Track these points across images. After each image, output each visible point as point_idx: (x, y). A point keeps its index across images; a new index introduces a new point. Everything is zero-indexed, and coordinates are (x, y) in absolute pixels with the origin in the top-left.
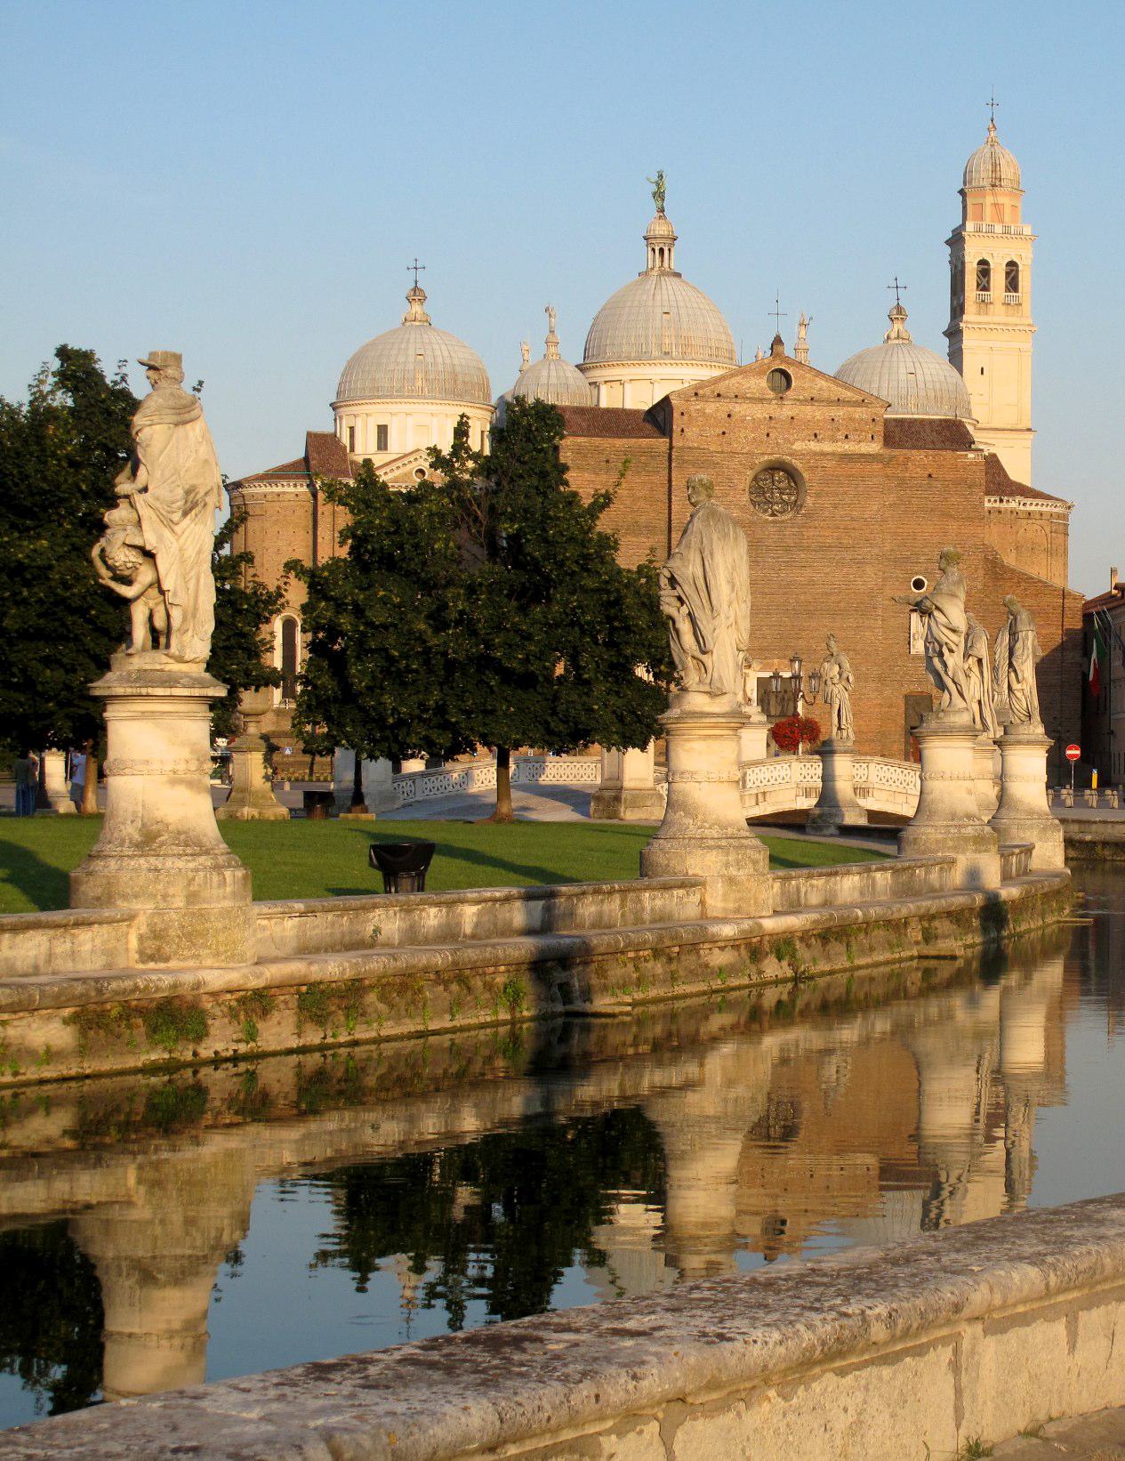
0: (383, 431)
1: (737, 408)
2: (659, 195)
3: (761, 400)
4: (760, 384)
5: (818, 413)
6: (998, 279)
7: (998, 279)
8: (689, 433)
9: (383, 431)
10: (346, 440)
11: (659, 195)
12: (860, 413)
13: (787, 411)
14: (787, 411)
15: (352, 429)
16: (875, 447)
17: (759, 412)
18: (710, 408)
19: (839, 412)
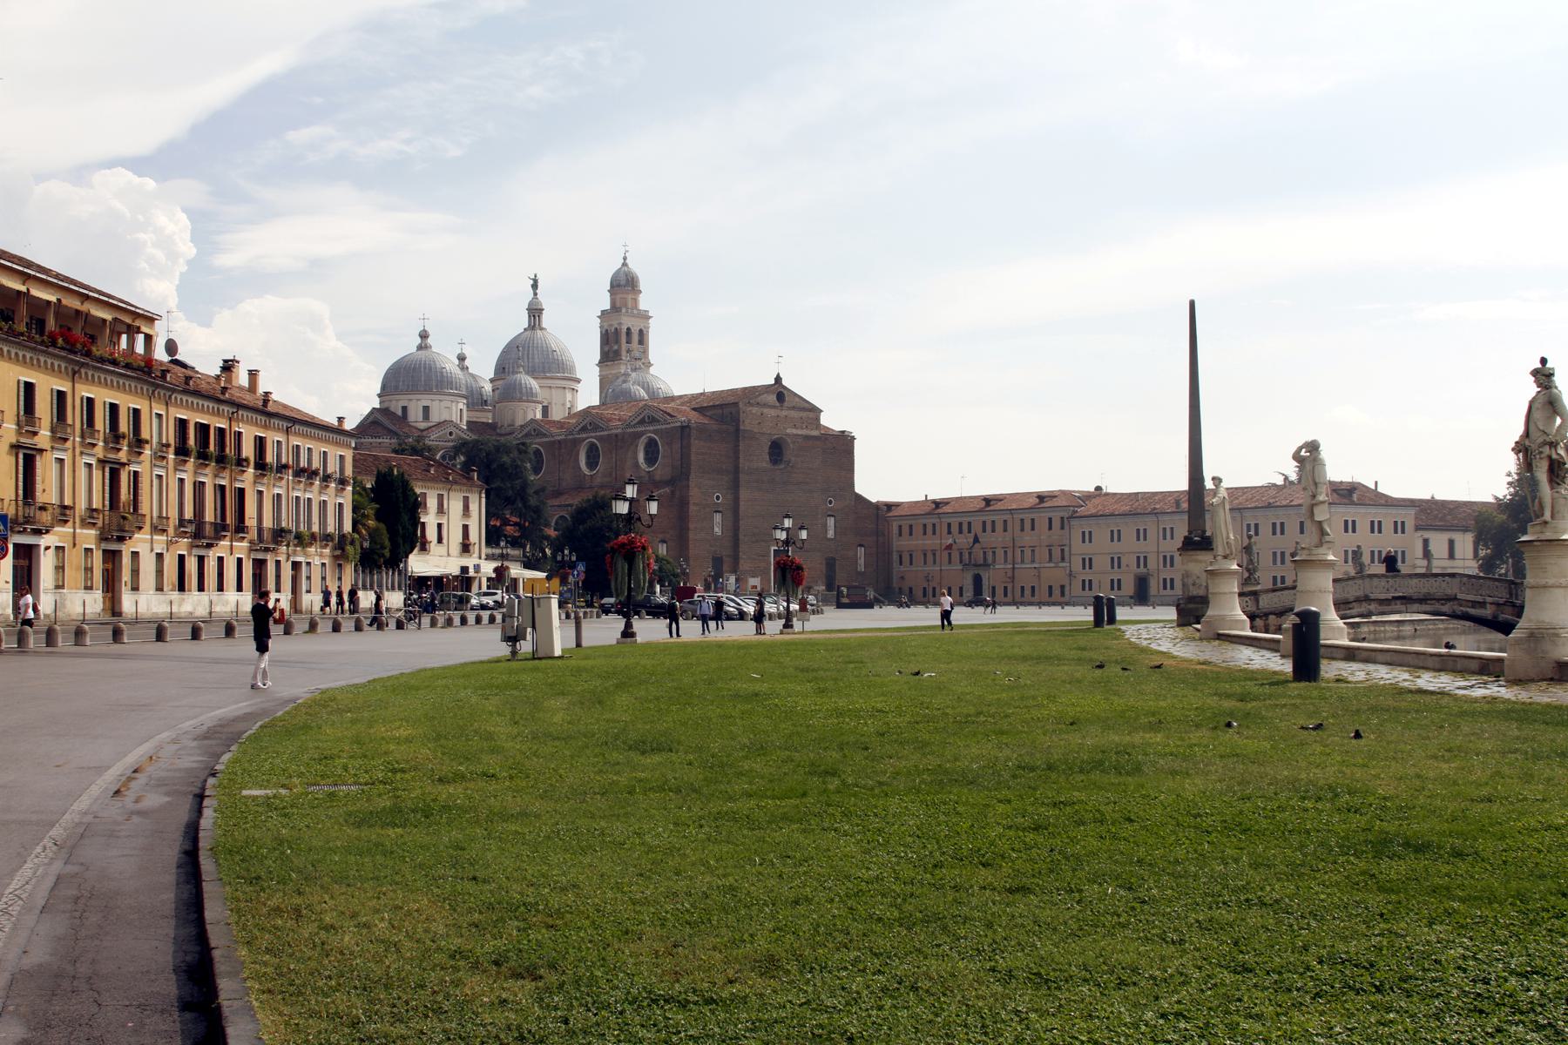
0: (426, 409)
1: (766, 411)
2: (535, 286)
3: (774, 407)
4: (772, 398)
5: (793, 414)
6: (635, 338)
7: (635, 338)
8: (747, 424)
9: (426, 409)
10: (399, 413)
11: (535, 286)
12: (811, 415)
13: (784, 413)
14: (784, 413)
15: (405, 409)
16: (815, 433)
17: (773, 412)
18: (755, 410)
19: (804, 414)
